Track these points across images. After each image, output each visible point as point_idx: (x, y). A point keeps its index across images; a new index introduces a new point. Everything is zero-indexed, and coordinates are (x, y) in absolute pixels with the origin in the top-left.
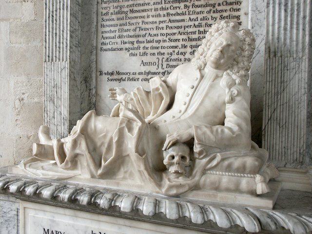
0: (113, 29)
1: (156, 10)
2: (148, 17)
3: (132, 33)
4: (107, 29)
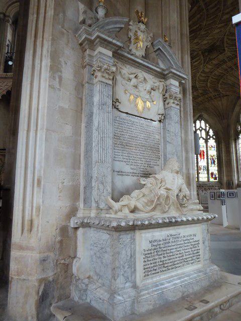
3: (127, 155)
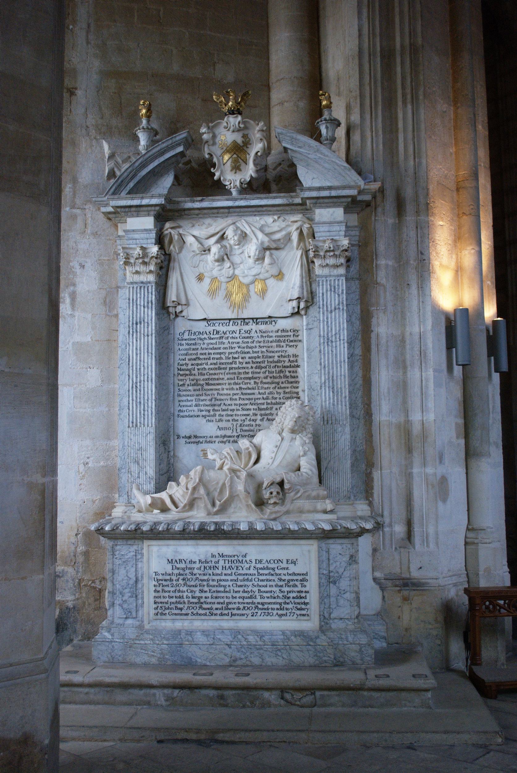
0: (189, 398)
1: (229, 384)
2: (223, 389)
3: (208, 403)
4: (184, 398)
